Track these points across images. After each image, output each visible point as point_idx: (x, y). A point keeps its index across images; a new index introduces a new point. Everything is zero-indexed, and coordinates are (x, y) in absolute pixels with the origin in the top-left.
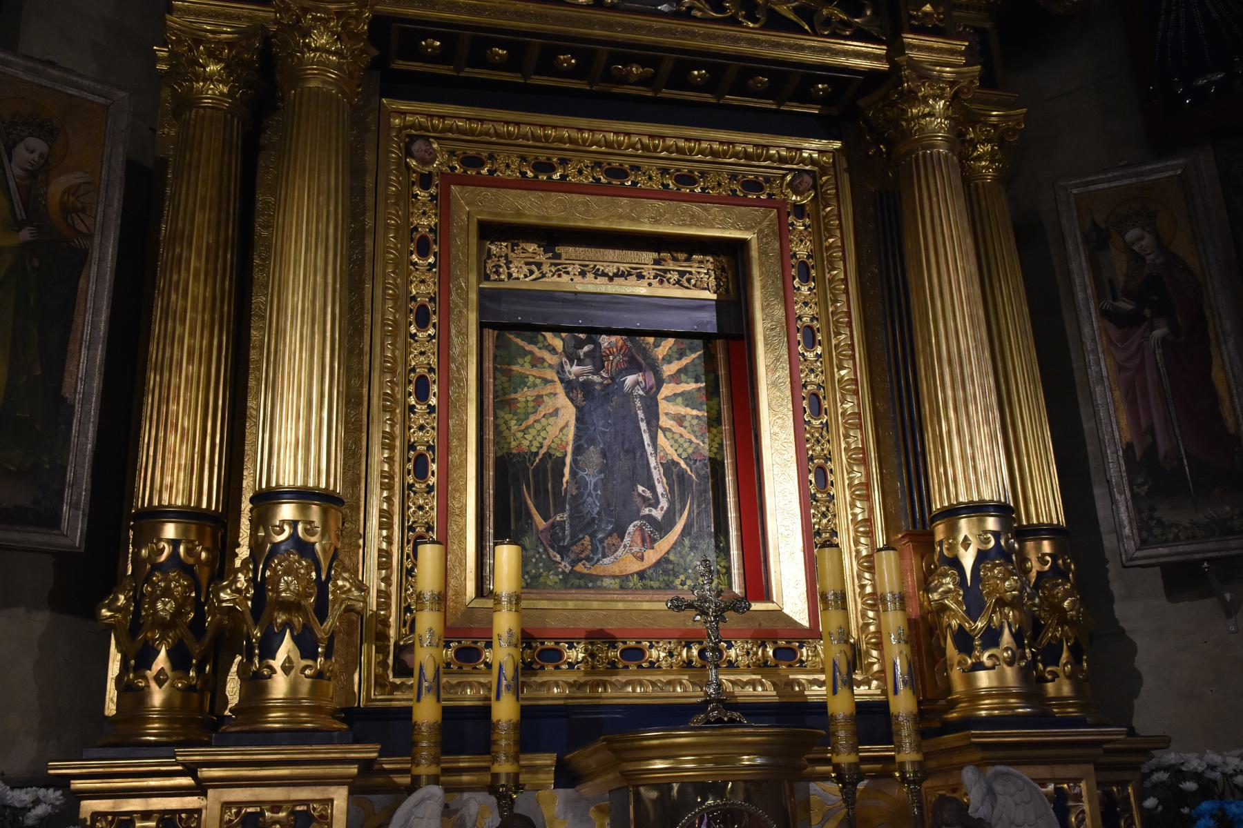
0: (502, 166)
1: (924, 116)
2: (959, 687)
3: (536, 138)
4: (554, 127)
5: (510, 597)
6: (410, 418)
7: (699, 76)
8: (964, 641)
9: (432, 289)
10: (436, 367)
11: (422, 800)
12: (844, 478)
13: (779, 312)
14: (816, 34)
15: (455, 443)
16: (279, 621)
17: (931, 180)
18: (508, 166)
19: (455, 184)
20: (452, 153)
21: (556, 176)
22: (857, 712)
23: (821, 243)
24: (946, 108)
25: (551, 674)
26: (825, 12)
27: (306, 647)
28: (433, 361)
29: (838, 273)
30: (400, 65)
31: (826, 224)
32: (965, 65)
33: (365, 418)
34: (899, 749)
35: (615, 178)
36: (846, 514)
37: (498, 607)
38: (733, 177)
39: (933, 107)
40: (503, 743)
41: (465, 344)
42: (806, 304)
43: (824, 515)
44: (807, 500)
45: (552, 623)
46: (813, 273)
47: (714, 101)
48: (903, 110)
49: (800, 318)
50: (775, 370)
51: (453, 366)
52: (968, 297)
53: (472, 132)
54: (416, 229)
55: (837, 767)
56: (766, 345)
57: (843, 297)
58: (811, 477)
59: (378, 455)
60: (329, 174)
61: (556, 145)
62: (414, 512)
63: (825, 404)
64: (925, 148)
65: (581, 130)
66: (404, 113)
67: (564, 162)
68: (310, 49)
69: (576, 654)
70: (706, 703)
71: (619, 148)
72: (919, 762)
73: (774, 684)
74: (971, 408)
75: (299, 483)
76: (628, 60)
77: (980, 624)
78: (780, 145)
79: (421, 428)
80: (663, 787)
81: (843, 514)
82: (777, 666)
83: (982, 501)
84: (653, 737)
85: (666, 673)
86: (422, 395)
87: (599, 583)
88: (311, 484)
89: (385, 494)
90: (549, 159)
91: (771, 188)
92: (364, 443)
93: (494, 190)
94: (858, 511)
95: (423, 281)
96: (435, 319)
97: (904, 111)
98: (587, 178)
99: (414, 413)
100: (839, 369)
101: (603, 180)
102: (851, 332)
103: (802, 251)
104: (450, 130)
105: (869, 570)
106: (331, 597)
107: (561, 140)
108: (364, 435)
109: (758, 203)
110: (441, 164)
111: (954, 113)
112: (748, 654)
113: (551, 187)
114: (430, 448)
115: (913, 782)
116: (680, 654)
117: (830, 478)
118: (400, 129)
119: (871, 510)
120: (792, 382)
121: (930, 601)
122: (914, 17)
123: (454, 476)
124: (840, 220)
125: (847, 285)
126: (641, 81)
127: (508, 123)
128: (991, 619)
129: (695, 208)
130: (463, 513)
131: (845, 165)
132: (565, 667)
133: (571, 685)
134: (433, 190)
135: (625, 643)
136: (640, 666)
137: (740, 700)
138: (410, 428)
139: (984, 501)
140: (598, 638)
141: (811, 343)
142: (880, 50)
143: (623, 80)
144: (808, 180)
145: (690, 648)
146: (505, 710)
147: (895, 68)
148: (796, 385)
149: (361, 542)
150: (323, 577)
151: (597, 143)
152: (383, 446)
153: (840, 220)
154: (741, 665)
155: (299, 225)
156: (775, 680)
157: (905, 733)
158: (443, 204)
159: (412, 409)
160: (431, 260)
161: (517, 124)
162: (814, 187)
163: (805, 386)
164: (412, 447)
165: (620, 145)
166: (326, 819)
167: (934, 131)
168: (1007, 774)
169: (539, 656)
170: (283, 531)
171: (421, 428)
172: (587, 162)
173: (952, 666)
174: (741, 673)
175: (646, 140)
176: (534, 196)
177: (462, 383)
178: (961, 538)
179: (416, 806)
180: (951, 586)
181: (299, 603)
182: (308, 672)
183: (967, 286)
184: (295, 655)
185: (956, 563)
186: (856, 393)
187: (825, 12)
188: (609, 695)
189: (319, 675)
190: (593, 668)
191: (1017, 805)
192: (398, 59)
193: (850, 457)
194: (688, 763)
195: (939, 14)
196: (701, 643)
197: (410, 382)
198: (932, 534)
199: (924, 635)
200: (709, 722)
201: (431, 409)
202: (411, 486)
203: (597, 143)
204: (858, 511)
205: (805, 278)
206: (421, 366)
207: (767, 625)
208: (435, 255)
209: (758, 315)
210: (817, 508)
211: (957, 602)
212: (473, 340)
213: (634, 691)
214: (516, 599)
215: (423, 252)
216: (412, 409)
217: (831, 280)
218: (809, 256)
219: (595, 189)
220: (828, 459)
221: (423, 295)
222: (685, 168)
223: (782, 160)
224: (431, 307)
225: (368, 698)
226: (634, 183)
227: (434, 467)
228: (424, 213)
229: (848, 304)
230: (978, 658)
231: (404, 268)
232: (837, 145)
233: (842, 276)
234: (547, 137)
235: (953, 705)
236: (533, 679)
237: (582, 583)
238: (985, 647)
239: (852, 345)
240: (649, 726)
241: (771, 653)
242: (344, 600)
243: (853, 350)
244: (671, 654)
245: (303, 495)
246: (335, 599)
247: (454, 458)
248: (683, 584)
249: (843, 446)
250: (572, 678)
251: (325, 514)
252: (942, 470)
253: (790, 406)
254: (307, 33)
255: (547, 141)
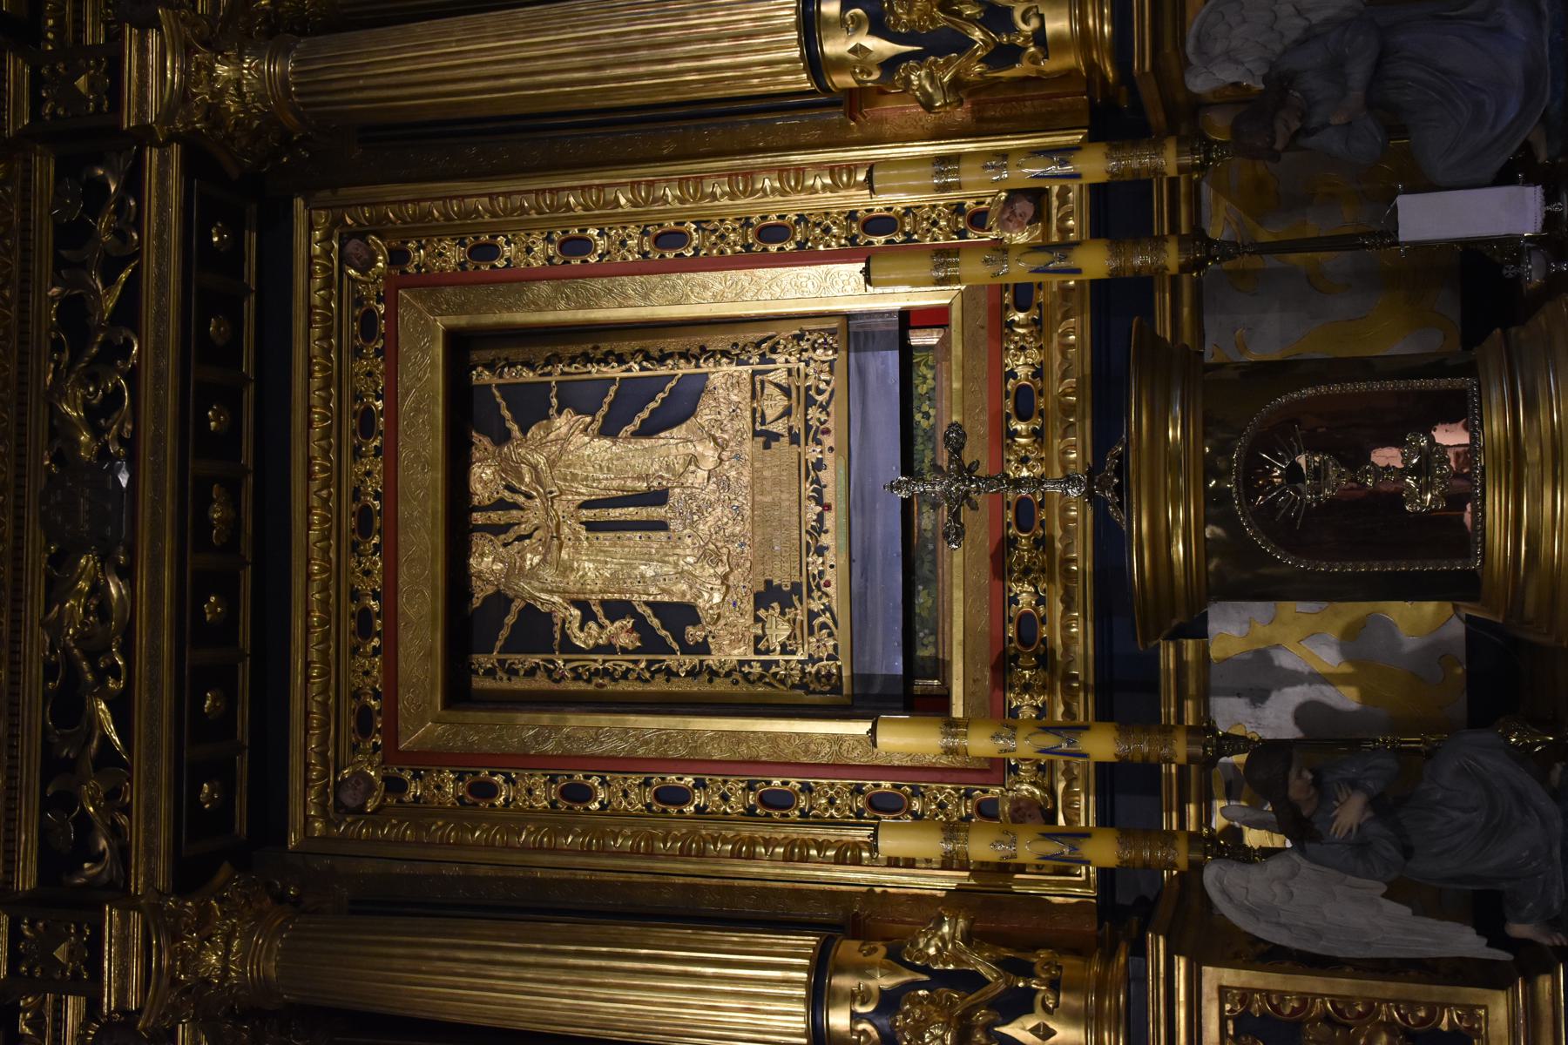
0: (368, 680)
1: (240, 94)
2: (1070, 60)
3: (325, 638)
4: (308, 614)
5: (946, 735)
6: (712, 813)
7: (217, 419)
8: (1004, 55)
9: (539, 779)
10: (643, 777)
11: (1224, 892)
12: (771, 200)
13: (544, 288)
14: (138, 254)
15: (743, 751)
16: (984, 1041)
17: (335, 86)
18: (367, 673)
19: (397, 745)
20: (355, 748)
21: (374, 605)
22: (1106, 236)
23: (442, 227)
24: (226, 60)
25: (1052, 630)
26: (107, 238)
27: (1019, 1005)
28: (635, 780)
29: (481, 204)
30: (241, 826)
31: (414, 218)
32: (159, 29)
33: (714, 881)
34: (1158, 172)
35: (372, 523)
36: (824, 199)
37: (961, 751)
38: (357, 353)
39: (228, 81)
40: (1146, 749)
41: (611, 733)
42: (529, 250)
43: (827, 230)
44: (805, 256)
45: (983, 623)
46: (485, 238)
47: (252, 387)
48: (236, 124)
49: (550, 259)
50: (628, 297)
51: (641, 752)
52: (500, 37)
53: (324, 725)
54: (460, 799)
55: (1183, 268)
56: (590, 307)
57: (517, 200)
58: (773, 248)
59: (766, 869)
60: (388, 956)
61: (333, 609)
62: (838, 810)
63: (670, 225)
64: (288, 94)
65: (309, 575)
66: (307, 817)
67: (355, 595)
68: (226, 970)
69: (1024, 594)
70: (1090, 494)
71: (330, 520)
72: (1179, 143)
73: (1066, 317)
74: (663, 37)
75: (801, 1008)
76: (203, 524)
77: (977, 35)
78: (308, 290)
79: (725, 798)
80: (1209, 548)
81: (825, 203)
82: (1039, 306)
83: (798, 26)
84: (1139, 563)
85: (1049, 467)
86: (682, 796)
87: (929, 535)
88: (801, 992)
89: (813, 852)
90: (353, 616)
91: (368, 299)
92: (748, 883)
93: (401, 691)
94: (819, 183)
95: (530, 792)
96: (579, 777)
97: (238, 123)
98: (375, 563)
99: (705, 807)
100: (619, 205)
101: (376, 540)
102: (564, 189)
103: (454, 255)
104: (323, 755)
105: (900, 175)
106: (951, 967)
107: (324, 603)
108: (737, 883)
109: (392, 315)
110: (370, 764)
111: (232, 49)
112: (1023, 349)
113: (390, 612)
114: (751, 787)
115: (1207, 153)
116: (1024, 447)
117: (773, 219)
118: (329, 823)
119: (817, 166)
120: (641, 274)
121: (945, 104)
122: (98, 106)
123: (787, 753)
124: (406, 202)
125: (499, 194)
126: (234, 501)
127: (307, 678)
128: (971, 20)
129: (407, 405)
130: (838, 739)
131: (326, 194)
132: (1041, 608)
133: (1068, 608)
134: (407, 776)
135: (1009, 525)
136: (1041, 505)
137: (1088, 370)
138: (725, 813)
139: (797, 22)
140: (1001, 563)
141: (585, 245)
142: (152, 156)
143: (234, 526)
144: (353, 245)
145: (1016, 433)
146: (1102, 745)
147: (172, 138)
148: (644, 267)
149: (878, 890)
150: (925, 978)
151: (326, 551)
152: (752, 856)
153: (406, 202)
154: (1038, 358)
155: (460, 999)
156: (1059, 317)
157: (1135, 164)
158: (427, 760)
159: (700, 810)
160: (498, 779)
161: (307, 665)
162: (362, 236)
163: (645, 255)
164: (750, 811)
165: (324, 520)
166: (1246, 994)
167: (261, 80)
168: (1198, 39)
169: (1028, 646)
170: (864, 1032)
171: (725, 798)
172: (354, 564)
173: (1038, 71)
174: (1049, 356)
175: (315, 486)
176: (405, 636)
177: (666, 738)
178: (852, 56)
179: (1231, 900)
180: (923, 73)
181: (960, 1017)
182: (1050, 1003)
183: (483, 39)
184: (1031, 1022)
185: (890, 65)
186: (650, 184)
187: (107, 238)
188: (1081, 558)
189: (1055, 986)
190: (1043, 571)
191: (1244, 21)
192: (231, 839)
193: (744, 193)
194: (1177, 515)
195: (89, 67)
196: (1008, 417)
197: (664, 811)
198: (851, 90)
199: (992, 107)
200: (1120, 504)
201: (700, 784)
202: (803, 814)
203: (326, 551)
204: (819, 183)
205: (491, 251)
206: (641, 796)
207: (982, 317)
208: (493, 774)
209: (549, 317)
210: (816, 241)
211: (947, 64)
212: (605, 720)
213: (1075, 520)
214: (951, 725)
215: (491, 791)
216: (700, 810)
217: (494, 215)
218: (462, 244)
219: (389, 551)
220: (747, 223)
221: (548, 791)
222: (350, 424)
223: (327, 284)
224: (562, 781)
225: (1085, 884)
226: (377, 496)
227: (777, 782)
228: (438, 787)
229: (524, 192)
230: (1027, 38)
231: (515, 818)
232: (299, 203)
233: (486, 200)
234: (323, 622)
235: (1092, 66)
236: (1059, 657)
237: (929, 557)
238: (1011, 28)
239: (583, 188)
240: (1123, 571)
241: (1020, 316)
242: (954, 944)
243: (590, 187)
244: (1024, 461)
245: (818, 998)
246: (957, 961)
247: (763, 752)
248: (927, 416)
249: (725, 201)
250: (1059, 607)
251: (841, 970)
252: (755, 81)
253: (674, 276)
254: (207, 982)
255: (329, 622)
